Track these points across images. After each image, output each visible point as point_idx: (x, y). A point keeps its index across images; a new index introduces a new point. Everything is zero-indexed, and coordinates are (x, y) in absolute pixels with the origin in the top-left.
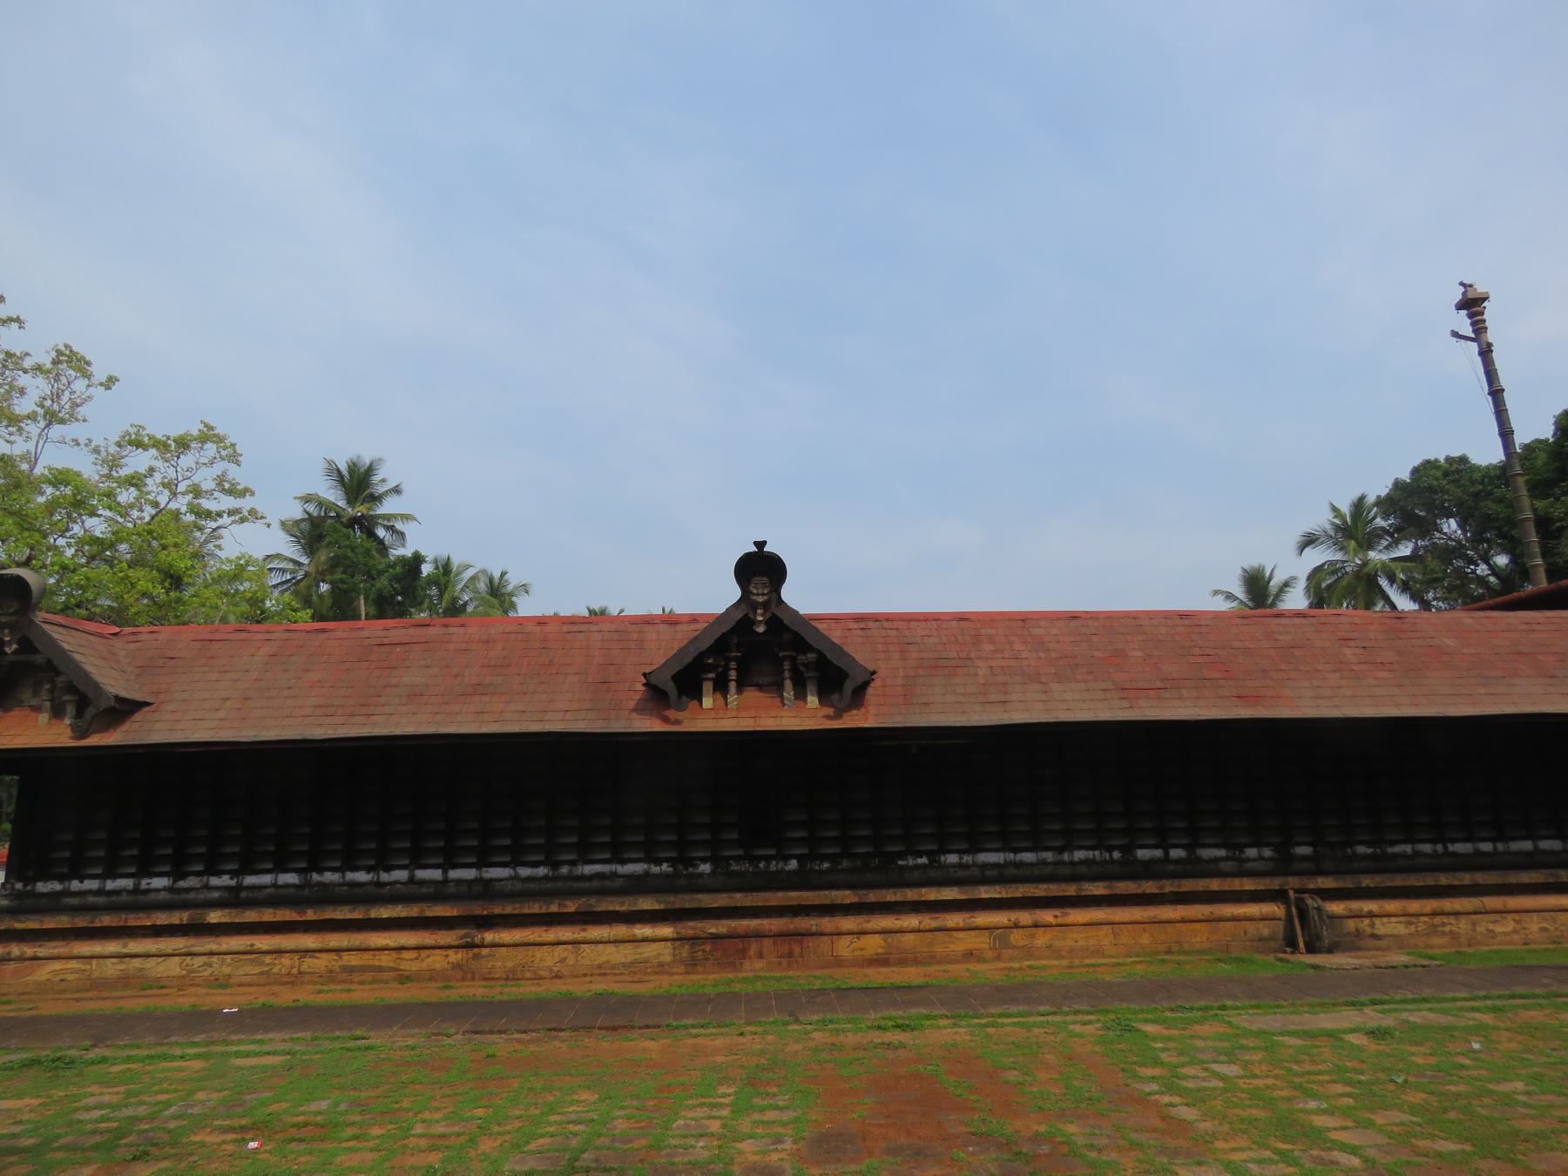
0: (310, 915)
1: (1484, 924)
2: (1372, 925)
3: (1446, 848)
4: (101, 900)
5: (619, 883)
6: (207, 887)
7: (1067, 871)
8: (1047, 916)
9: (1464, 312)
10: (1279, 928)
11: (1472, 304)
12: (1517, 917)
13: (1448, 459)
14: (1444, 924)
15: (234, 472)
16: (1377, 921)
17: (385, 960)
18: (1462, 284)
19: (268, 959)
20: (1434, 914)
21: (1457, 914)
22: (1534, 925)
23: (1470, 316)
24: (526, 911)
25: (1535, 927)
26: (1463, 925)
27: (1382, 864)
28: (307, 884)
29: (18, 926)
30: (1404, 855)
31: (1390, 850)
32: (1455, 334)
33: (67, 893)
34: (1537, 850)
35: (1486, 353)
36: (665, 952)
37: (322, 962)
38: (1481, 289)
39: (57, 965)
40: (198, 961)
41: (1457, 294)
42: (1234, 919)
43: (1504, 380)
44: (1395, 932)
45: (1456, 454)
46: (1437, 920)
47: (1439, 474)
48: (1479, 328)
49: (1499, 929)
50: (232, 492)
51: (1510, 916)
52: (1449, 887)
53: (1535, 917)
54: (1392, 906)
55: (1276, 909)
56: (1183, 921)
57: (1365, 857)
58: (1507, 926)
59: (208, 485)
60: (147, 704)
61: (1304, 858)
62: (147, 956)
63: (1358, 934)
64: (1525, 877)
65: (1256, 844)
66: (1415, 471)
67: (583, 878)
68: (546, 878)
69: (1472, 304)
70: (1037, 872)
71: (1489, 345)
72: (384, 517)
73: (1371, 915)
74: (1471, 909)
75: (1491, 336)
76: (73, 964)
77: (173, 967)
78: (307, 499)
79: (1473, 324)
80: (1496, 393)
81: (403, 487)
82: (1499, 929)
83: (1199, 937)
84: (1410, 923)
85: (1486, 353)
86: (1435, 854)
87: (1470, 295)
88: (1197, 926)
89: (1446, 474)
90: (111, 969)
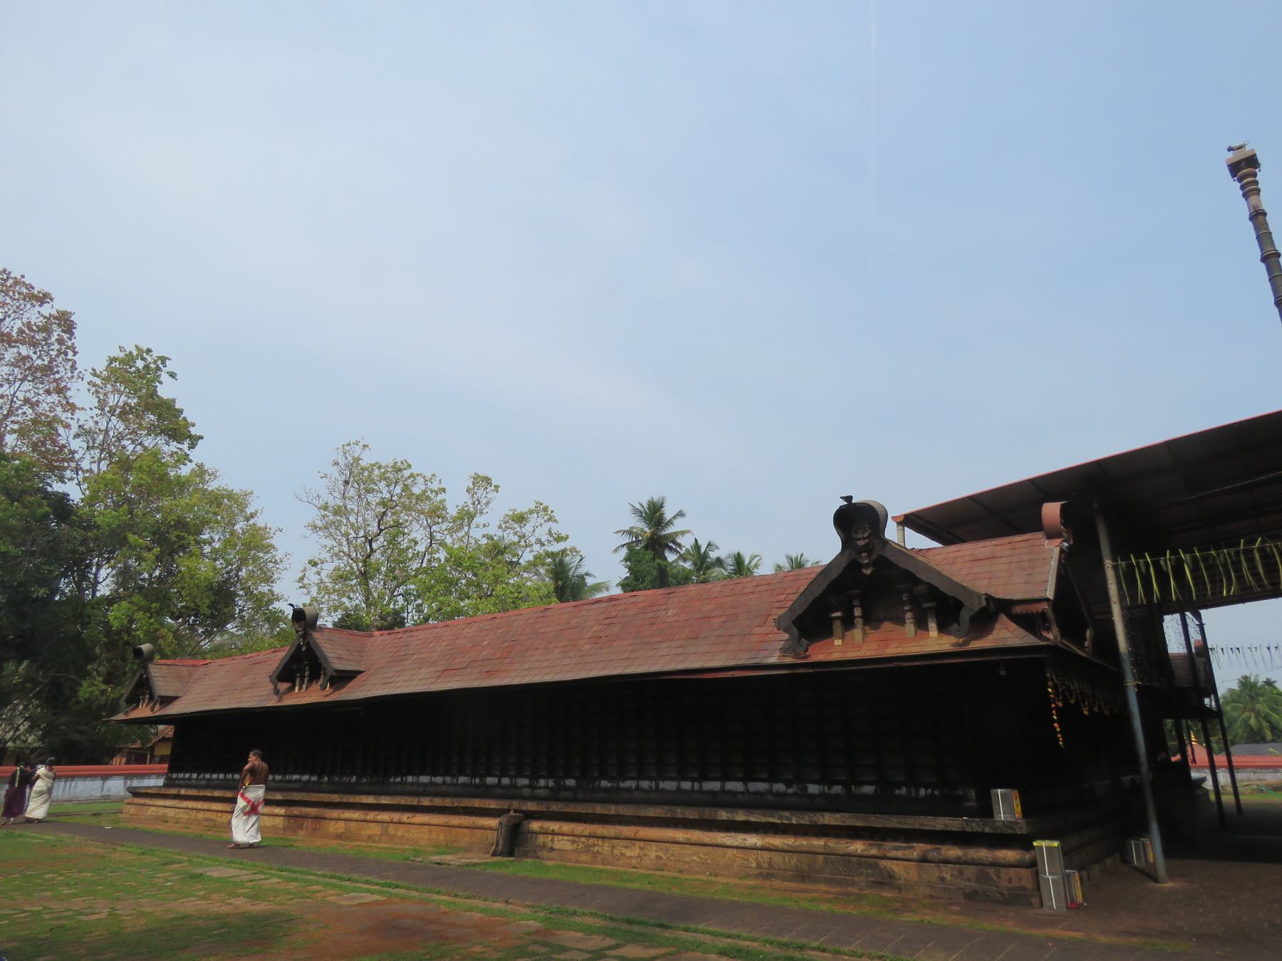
0: (201, 793)
1: (620, 848)
2: (552, 841)
3: (657, 785)
5: (299, 785)
7: (451, 790)
8: (405, 817)
11: (1244, 168)
12: (642, 844)
14: (594, 845)
15: (556, 528)
16: (556, 838)
17: (213, 816)
18: (1230, 149)
20: (590, 836)
21: (603, 838)
22: (653, 852)
24: (643, 814)
25: (653, 855)
26: (605, 848)
27: (614, 797)
30: (629, 790)
31: (622, 785)
34: (723, 791)
36: (279, 822)
37: (201, 815)
38: (1255, 146)
39: (152, 809)
42: (483, 828)
44: (565, 847)
46: (591, 841)
48: (1250, 190)
49: (629, 853)
50: (559, 539)
51: (638, 844)
52: (602, 815)
53: (654, 845)
54: (567, 827)
56: (460, 827)
57: (607, 790)
58: (633, 852)
59: (544, 538)
60: (175, 698)
61: (569, 789)
63: (544, 846)
64: (652, 812)
65: (547, 777)
67: (291, 782)
69: (1244, 168)
70: (429, 789)
72: (676, 534)
73: (554, 833)
74: (613, 834)
77: (171, 813)
78: (630, 532)
81: (685, 511)
82: (629, 853)
83: (465, 838)
84: (574, 842)
86: (650, 791)
88: (465, 831)
90: (161, 811)
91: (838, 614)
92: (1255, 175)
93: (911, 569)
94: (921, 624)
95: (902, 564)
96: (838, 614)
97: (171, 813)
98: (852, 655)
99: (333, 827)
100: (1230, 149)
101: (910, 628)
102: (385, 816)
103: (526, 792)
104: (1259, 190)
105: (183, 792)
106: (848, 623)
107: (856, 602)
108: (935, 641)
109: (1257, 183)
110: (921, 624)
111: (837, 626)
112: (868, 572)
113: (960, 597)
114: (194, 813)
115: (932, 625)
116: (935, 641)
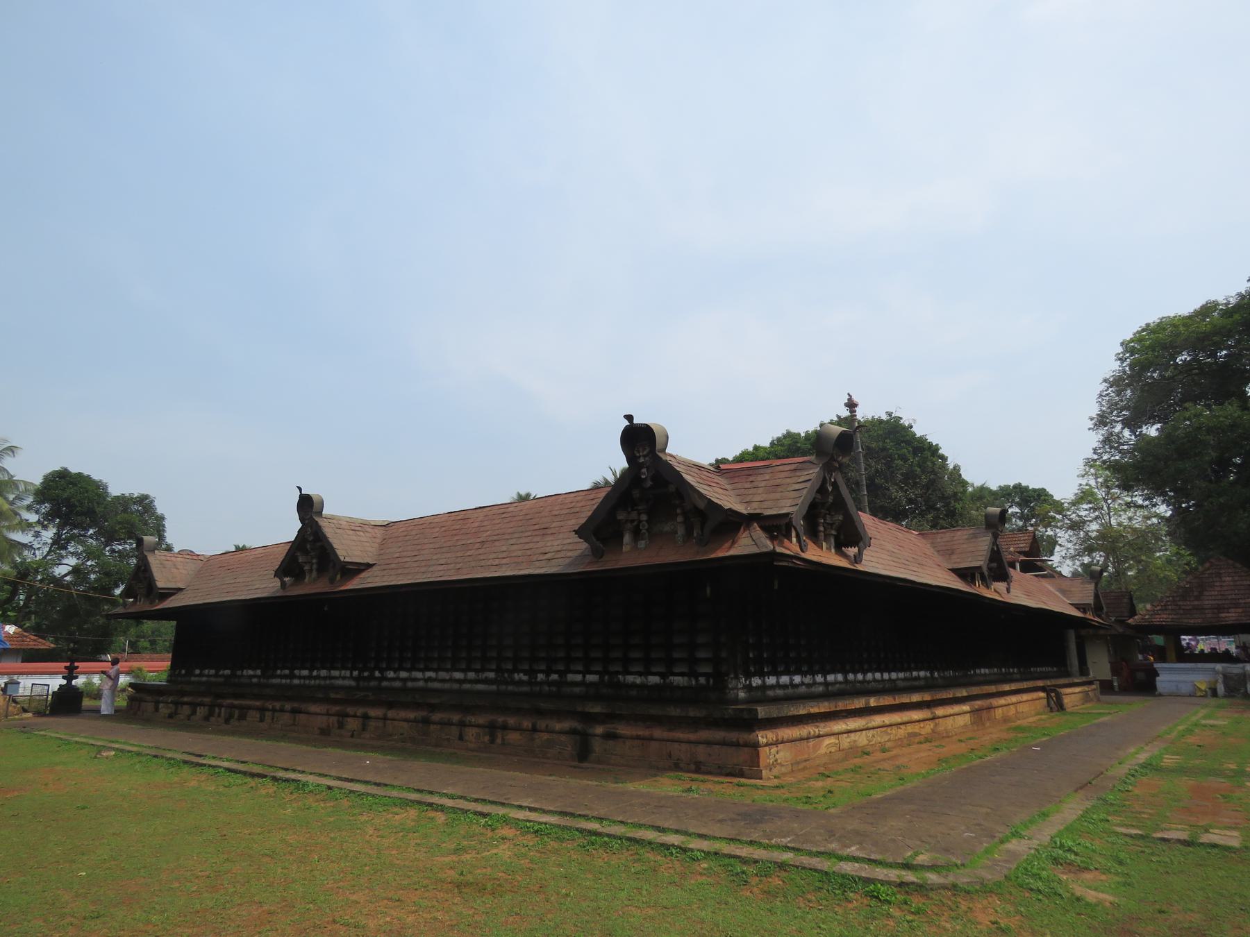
4: (780, 692)
5: (922, 683)
6: (815, 683)
10: (1045, 702)
19: (889, 730)
28: (846, 681)
29: (812, 711)
33: (764, 687)
37: (902, 732)
38: (855, 399)
39: (828, 741)
40: (871, 733)
55: (1042, 694)
62: (855, 731)
68: (905, 679)
76: (832, 740)
90: (846, 741)
97: (862, 739)
99: (999, 713)
102: (1014, 699)
103: (1015, 676)
105: (873, 702)
114: (894, 730)
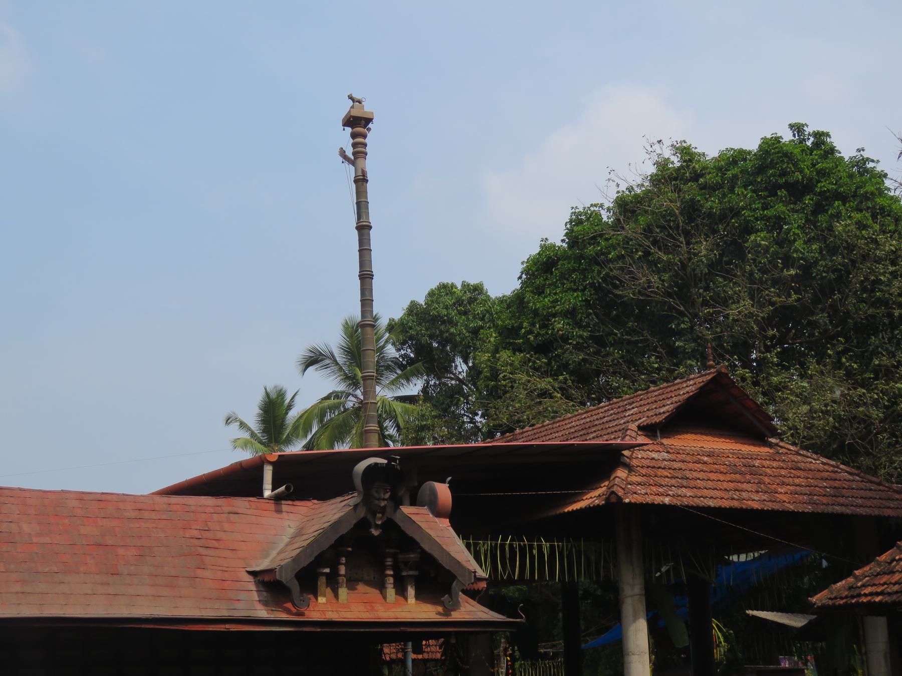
9: (349, 130)
11: (357, 123)
13: (466, 286)
18: (351, 97)
23: (354, 136)
32: (343, 153)
35: (361, 181)
38: (368, 108)
41: (344, 108)
43: (374, 217)
45: (473, 281)
47: (449, 301)
48: (359, 152)
66: (431, 294)
69: (357, 123)
71: (364, 173)
75: (370, 165)
79: (354, 145)
80: (363, 229)
85: (361, 181)
87: (355, 113)
89: (459, 302)
91: (327, 570)
92: (365, 136)
93: (417, 538)
94: (401, 591)
95: (410, 533)
96: (327, 570)
98: (333, 615)
100: (351, 97)
101: (391, 592)
104: (366, 154)
106: (333, 583)
107: (343, 560)
108: (414, 609)
109: (365, 145)
110: (401, 591)
111: (322, 580)
112: (375, 532)
113: (454, 570)
115: (411, 591)
116: (414, 609)
